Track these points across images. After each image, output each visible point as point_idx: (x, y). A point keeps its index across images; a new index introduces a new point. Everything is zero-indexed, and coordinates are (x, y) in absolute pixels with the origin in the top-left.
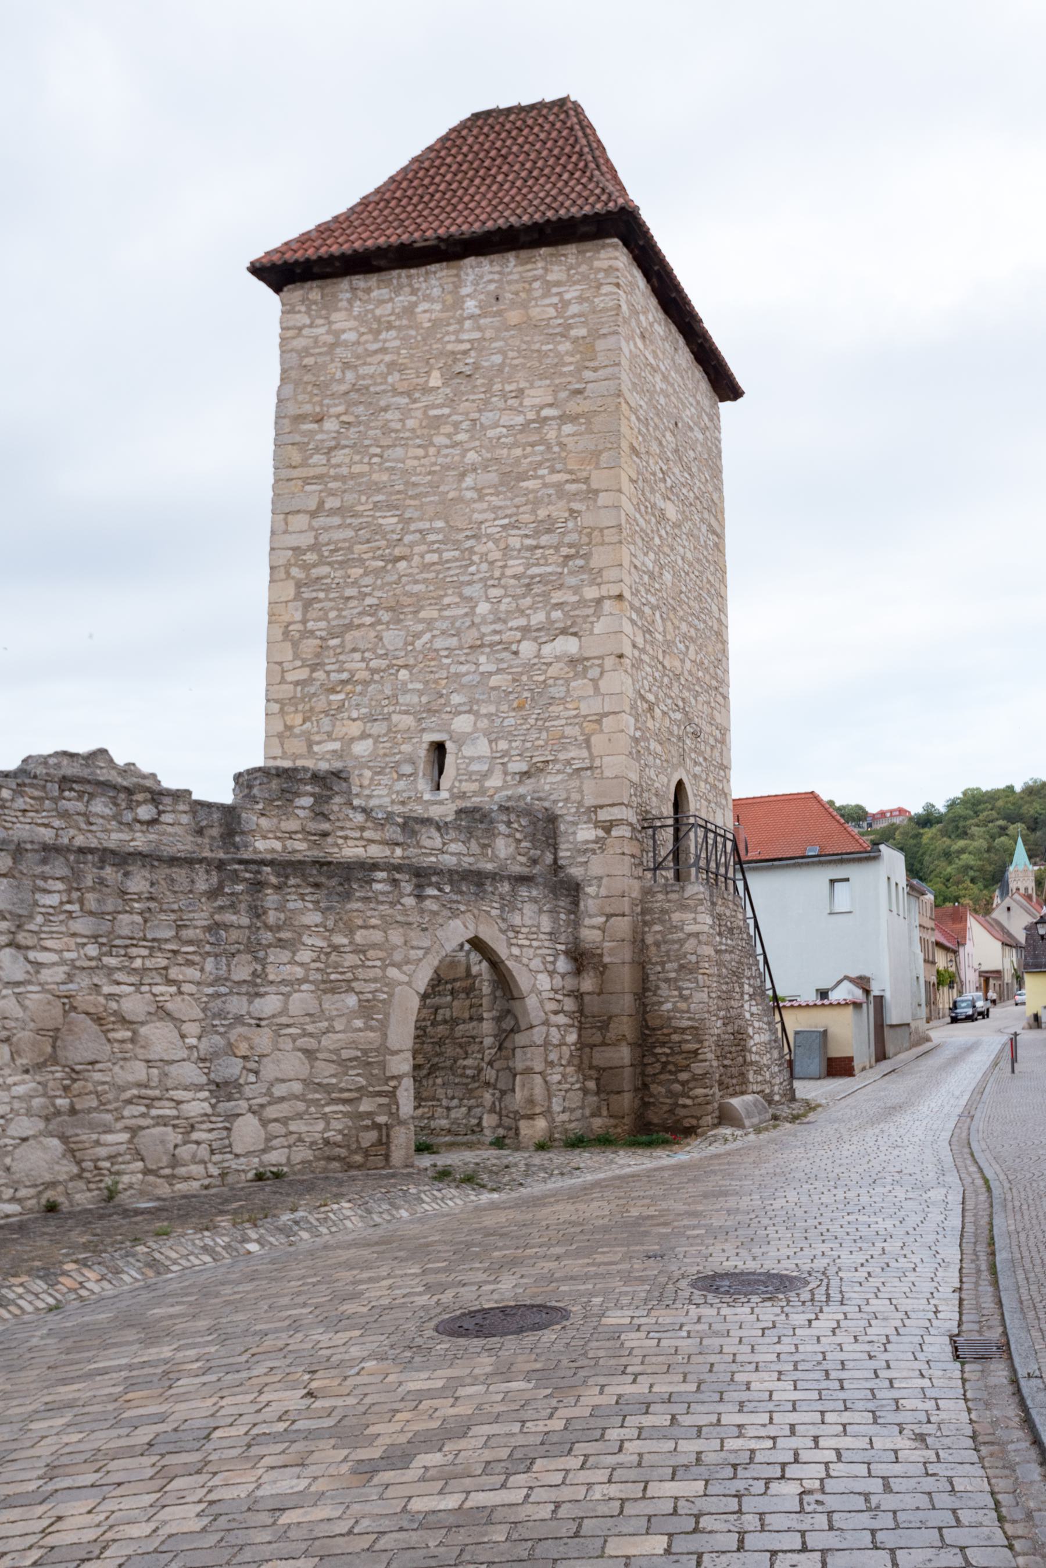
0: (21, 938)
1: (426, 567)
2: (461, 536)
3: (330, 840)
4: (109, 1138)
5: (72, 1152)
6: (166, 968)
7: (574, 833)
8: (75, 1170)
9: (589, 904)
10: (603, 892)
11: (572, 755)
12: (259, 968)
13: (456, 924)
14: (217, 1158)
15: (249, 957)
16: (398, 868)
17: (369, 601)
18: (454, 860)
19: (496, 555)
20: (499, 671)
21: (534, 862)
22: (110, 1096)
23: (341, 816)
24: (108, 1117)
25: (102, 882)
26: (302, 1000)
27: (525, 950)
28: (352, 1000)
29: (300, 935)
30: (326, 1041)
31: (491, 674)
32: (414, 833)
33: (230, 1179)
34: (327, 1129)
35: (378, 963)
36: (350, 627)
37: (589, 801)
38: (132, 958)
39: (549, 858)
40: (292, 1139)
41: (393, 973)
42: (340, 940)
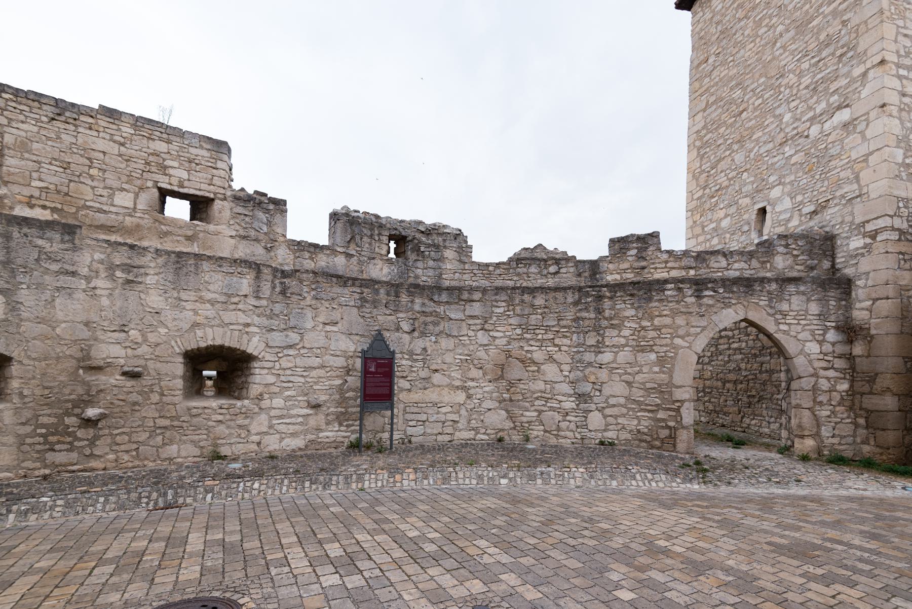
0: (486, 326)
3: (646, 270)
4: (527, 414)
5: (511, 417)
6: (553, 339)
7: (848, 244)
8: (512, 425)
9: (860, 292)
10: (870, 283)
11: (845, 190)
12: (600, 339)
13: (730, 311)
14: (579, 430)
15: (595, 333)
16: (682, 281)
18: (737, 274)
20: (796, 152)
21: (812, 268)
22: (528, 395)
23: (653, 257)
24: (527, 404)
25: (523, 301)
26: (624, 356)
27: (792, 327)
28: (653, 356)
29: (623, 322)
30: (638, 378)
31: (791, 156)
32: (704, 260)
33: (586, 441)
34: (639, 424)
35: (669, 336)
37: (858, 220)
38: (537, 335)
39: (826, 264)
40: (620, 427)
41: (678, 341)
42: (645, 323)
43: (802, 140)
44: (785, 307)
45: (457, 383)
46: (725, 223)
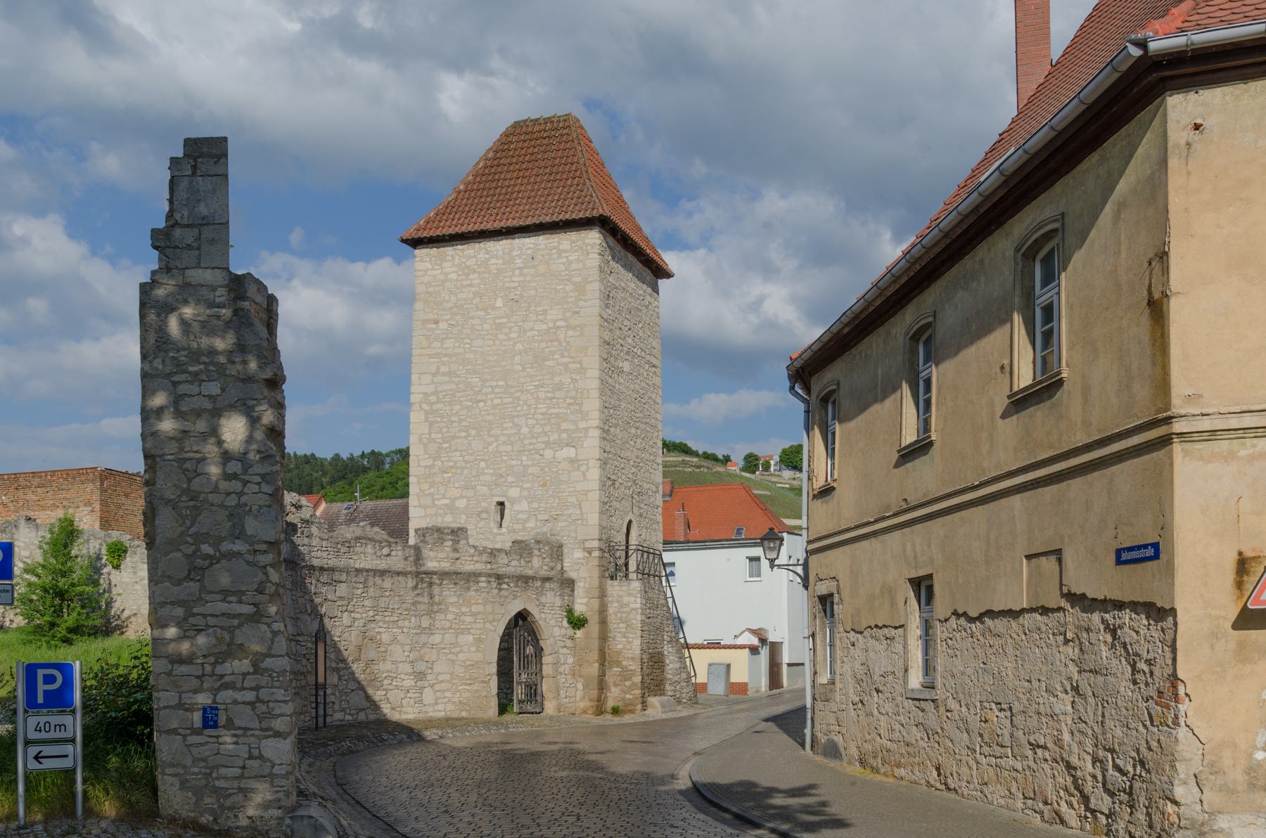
1: (494, 407)
2: (513, 390)
16: (490, 575)
17: (464, 423)
19: (533, 402)
26: (449, 637)
28: (470, 638)
36: (453, 437)
39: (559, 567)
42: (464, 609)
43: (537, 456)
44: (543, 600)
45: (334, 665)
46: (461, 503)
